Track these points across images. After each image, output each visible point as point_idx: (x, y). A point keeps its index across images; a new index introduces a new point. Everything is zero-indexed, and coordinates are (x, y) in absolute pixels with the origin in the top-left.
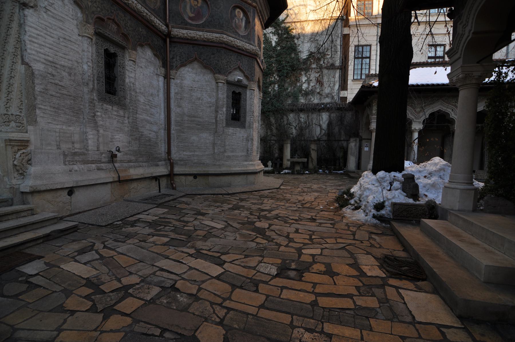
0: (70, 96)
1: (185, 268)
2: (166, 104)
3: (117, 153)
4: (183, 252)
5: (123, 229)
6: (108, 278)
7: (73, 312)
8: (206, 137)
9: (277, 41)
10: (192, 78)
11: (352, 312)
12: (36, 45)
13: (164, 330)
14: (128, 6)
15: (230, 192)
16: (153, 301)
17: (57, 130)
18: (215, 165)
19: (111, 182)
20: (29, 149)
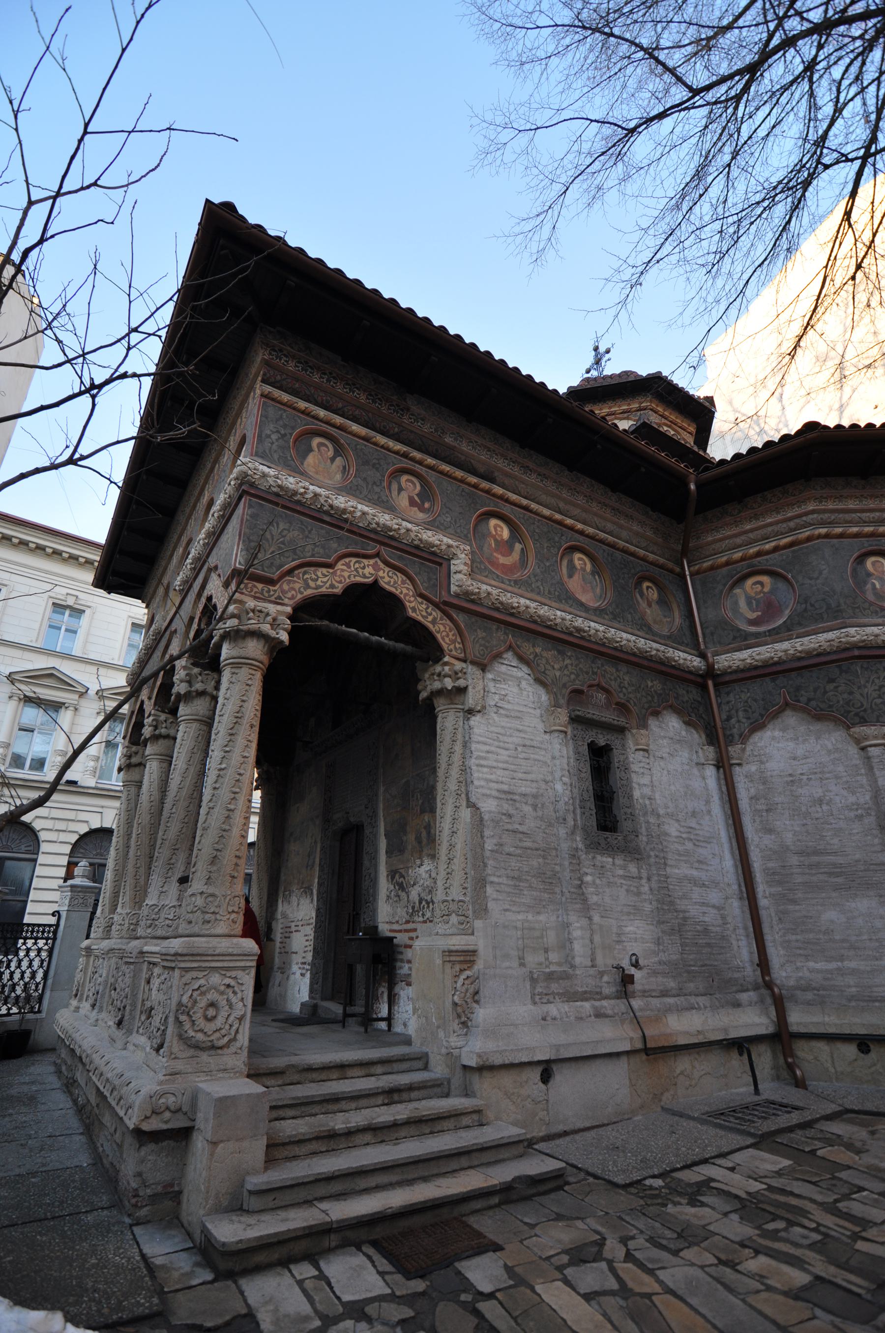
0: (537, 849)
2: (732, 831)
3: (633, 971)
5: (670, 1209)
12: (485, 770)
14: (621, 651)
17: (519, 924)
19: (627, 1053)
20: (476, 967)
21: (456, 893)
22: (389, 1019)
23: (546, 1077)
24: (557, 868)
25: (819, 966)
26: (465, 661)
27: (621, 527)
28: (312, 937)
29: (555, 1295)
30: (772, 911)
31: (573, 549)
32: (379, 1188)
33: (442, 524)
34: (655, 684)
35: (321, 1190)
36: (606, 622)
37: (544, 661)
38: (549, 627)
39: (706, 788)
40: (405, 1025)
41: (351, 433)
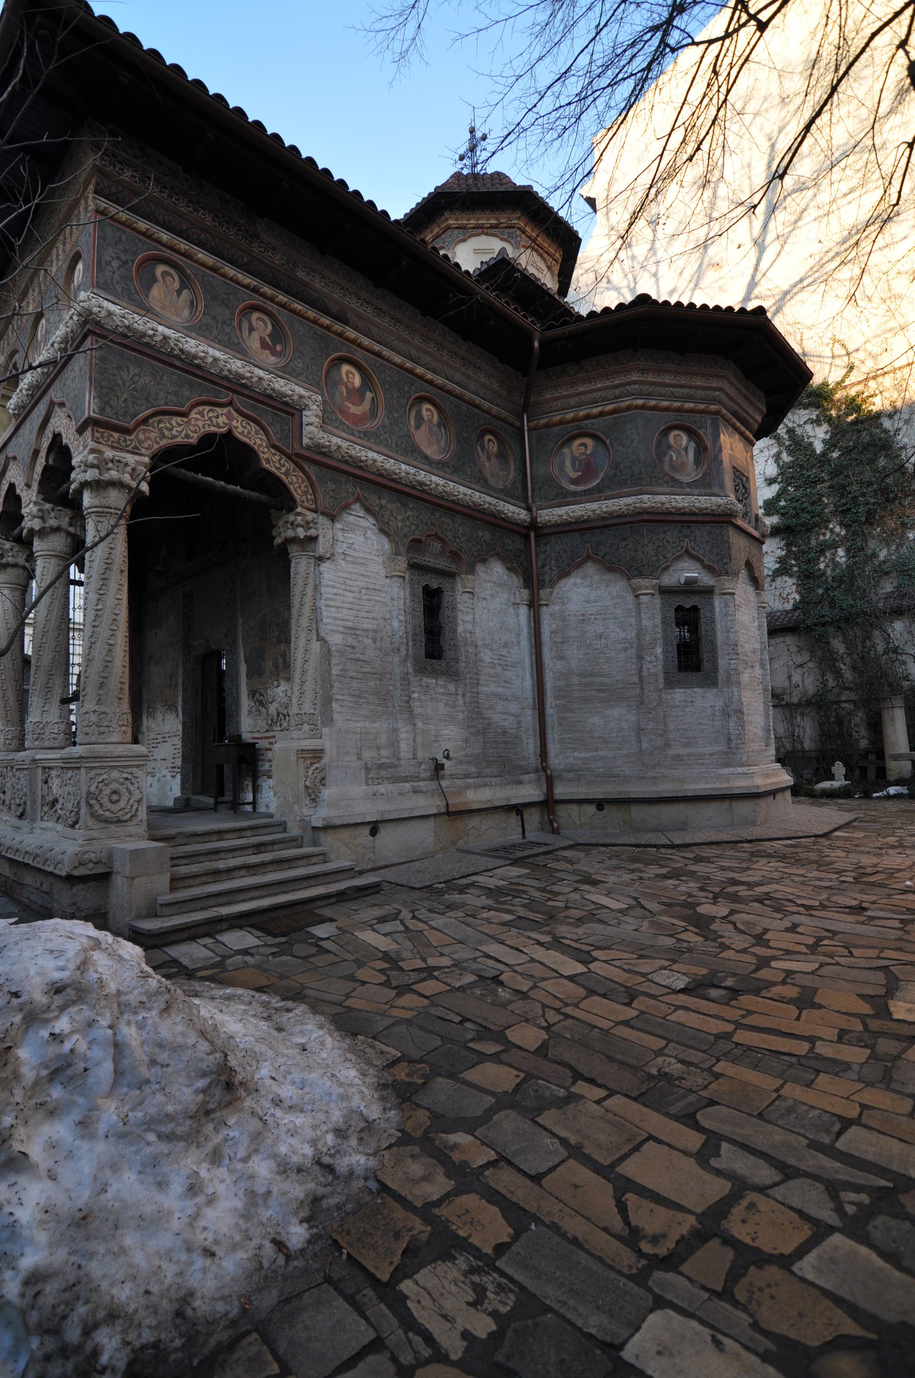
1: (523, 958)
3: (444, 761)
4: (529, 938)
5: (446, 896)
6: (410, 955)
7: (364, 983)
8: (620, 716)
9: (828, 437)
10: (586, 597)
11: (794, 1060)
12: (333, 609)
13: (466, 1020)
15: (678, 841)
16: (462, 989)
17: (358, 730)
18: (643, 778)
19: (434, 815)
20: (323, 761)
21: (307, 708)
22: (254, 803)
23: (374, 832)
24: (391, 688)
25: (580, 755)
26: (316, 512)
27: (469, 378)
28: (180, 746)
29: (368, 936)
30: (555, 718)
31: (422, 399)
32: (251, 899)
33: (294, 370)
34: (485, 535)
35: (213, 902)
36: (447, 476)
37: (388, 513)
38: (394, 480)
39: (518, 624)
40: (267, 806)
41: (197, 261)
